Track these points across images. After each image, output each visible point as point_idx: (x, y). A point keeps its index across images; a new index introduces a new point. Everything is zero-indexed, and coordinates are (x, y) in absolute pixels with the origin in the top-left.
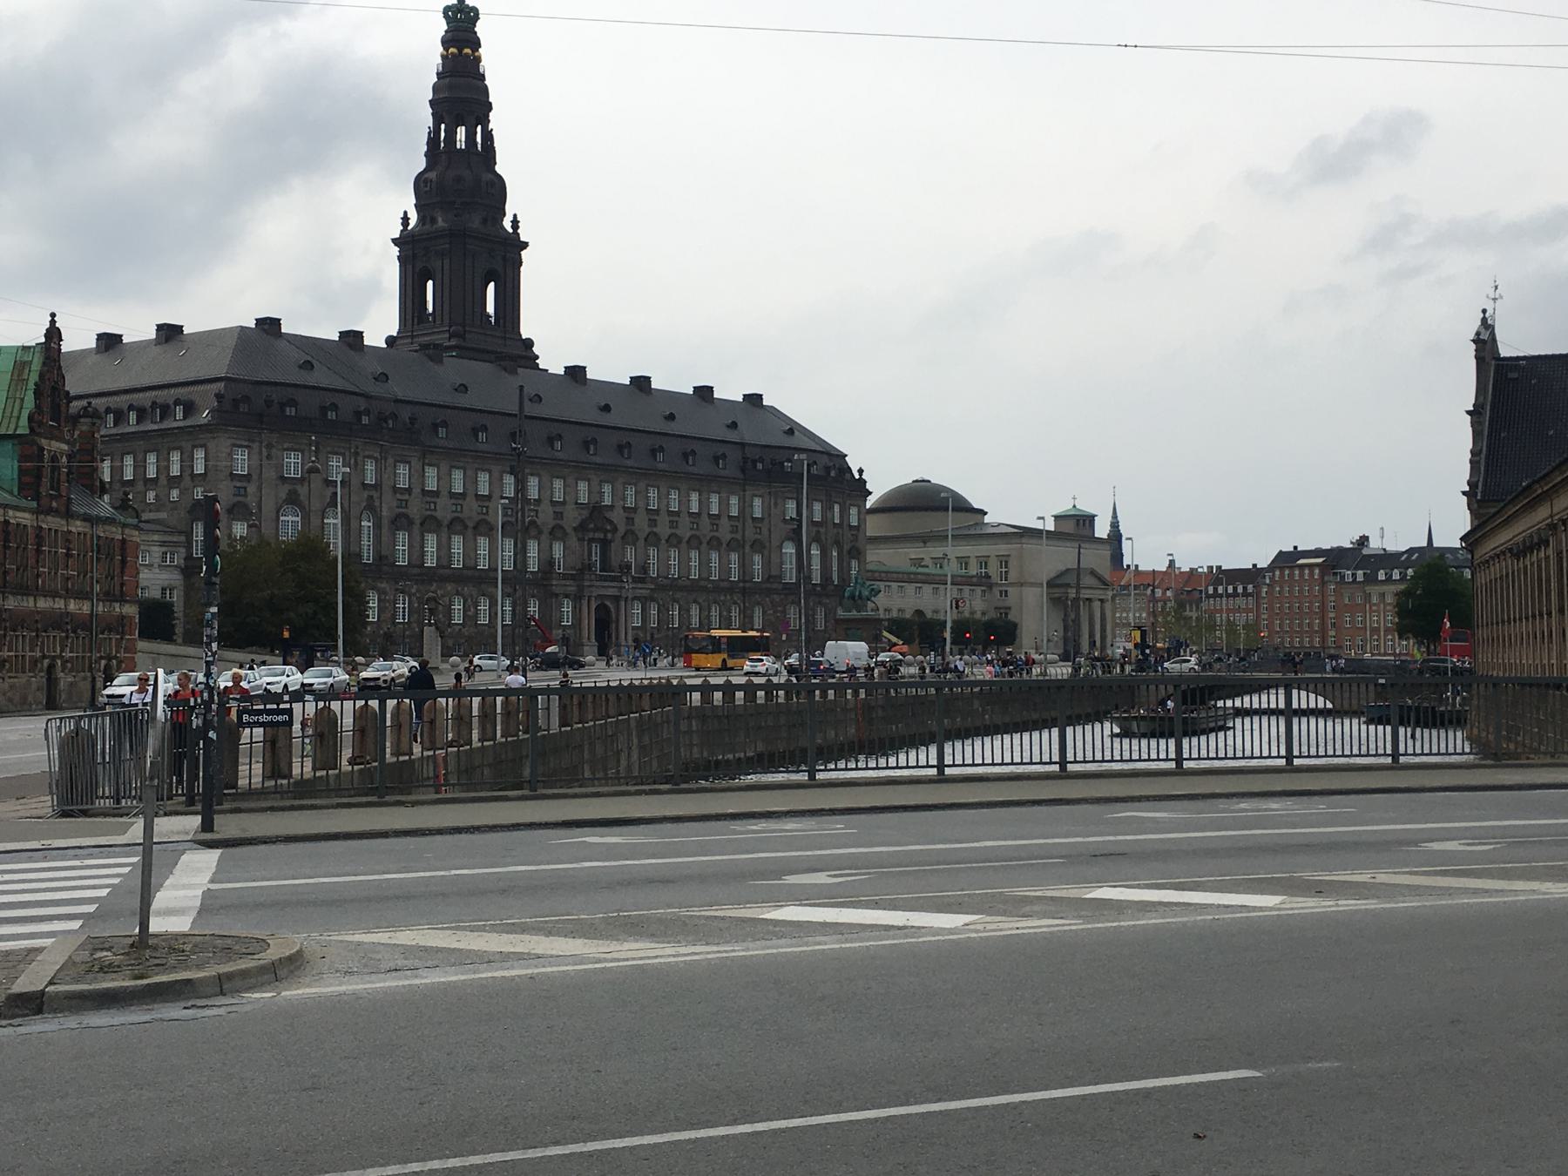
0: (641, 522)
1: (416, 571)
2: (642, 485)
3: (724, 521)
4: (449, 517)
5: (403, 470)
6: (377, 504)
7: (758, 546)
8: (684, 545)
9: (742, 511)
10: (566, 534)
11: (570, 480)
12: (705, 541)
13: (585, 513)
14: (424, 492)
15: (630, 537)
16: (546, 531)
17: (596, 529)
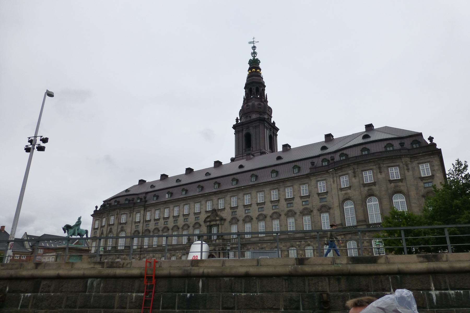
0: (241, 213)
1: (139, 250)
2: (241, 195)
3: (298, 201)
4: (154, 227)
5: (138, 215)
6: (125, 229)
7: (325, 209)
8: (268, 218)
9: (310, 192)
10: (200, 225)
11: (203, 202)
12: (283, 214)
13: (209, 214)
14: (146, 221)
15: (235, 220)
16: (191, 226)
17: (210, 222)
